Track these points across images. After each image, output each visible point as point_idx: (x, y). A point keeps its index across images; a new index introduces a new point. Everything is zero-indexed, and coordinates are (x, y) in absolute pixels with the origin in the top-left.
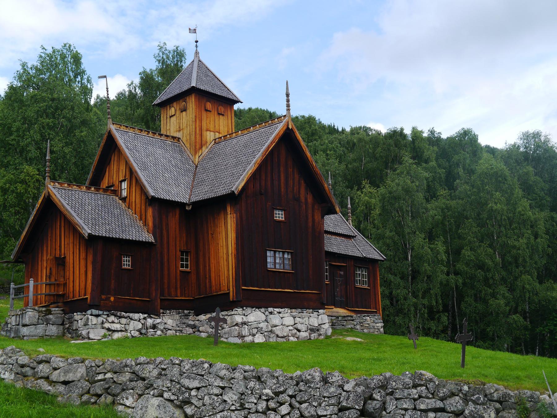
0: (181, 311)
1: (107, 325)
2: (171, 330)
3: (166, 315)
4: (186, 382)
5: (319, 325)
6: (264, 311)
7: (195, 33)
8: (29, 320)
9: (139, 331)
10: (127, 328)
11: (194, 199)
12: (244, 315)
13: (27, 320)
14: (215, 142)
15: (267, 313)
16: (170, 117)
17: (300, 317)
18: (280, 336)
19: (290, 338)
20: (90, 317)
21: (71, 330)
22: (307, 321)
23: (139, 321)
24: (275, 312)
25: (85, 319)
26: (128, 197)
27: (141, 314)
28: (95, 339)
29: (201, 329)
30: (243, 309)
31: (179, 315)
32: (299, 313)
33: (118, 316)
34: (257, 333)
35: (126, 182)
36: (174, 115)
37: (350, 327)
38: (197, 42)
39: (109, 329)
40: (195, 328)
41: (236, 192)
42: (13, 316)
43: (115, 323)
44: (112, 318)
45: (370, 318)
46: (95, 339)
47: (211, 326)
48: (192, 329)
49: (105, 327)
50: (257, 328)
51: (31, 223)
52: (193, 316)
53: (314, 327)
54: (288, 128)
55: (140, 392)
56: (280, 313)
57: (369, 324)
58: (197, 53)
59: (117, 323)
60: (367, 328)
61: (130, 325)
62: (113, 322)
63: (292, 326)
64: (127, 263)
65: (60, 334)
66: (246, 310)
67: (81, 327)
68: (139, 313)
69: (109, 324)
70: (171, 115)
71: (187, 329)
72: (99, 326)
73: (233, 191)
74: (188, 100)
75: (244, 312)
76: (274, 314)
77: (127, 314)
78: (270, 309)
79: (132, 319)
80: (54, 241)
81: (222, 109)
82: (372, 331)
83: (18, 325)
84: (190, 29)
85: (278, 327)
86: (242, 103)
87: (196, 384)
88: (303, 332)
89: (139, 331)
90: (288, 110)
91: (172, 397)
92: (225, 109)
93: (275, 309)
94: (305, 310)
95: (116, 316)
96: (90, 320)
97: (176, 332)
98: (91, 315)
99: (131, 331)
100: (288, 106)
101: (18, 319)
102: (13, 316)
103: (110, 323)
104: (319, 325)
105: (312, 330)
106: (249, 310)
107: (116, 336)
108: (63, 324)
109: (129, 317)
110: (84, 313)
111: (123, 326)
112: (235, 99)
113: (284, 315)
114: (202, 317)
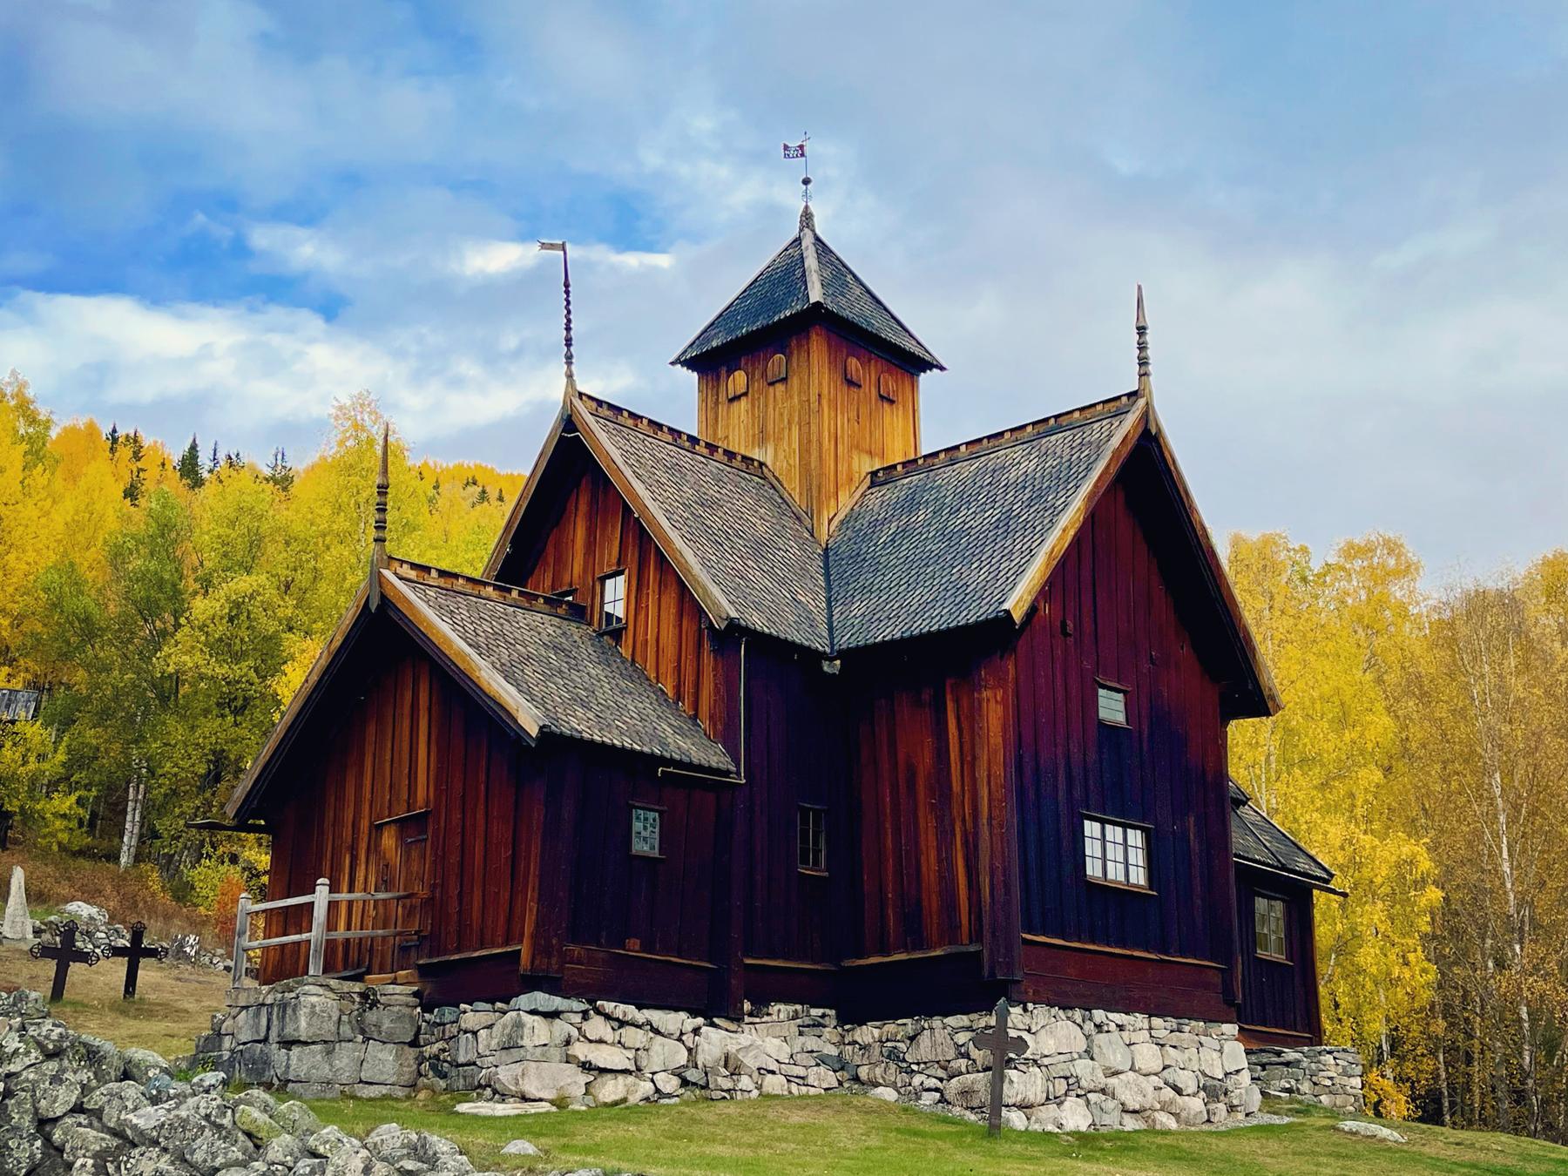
0: (799, 1007)
1: (581, 1050)
2: (773, 1072)
3: (757, 1020)
5: (1226, 1074)
6: (1079, 1020)
7: (802, 155)
8: (309, 1025)
9: (677, 1073)
10: (643, 1063)
11: (845, 641)
12: (1029, 1031)
13: (302, 1026)
14: (872, 482)
15: (1089, 1026)
16: (731, 400)
17: (1175, 1047)
18: (1131, 1109)
19: (1156, 1114)
20: (527, 1019)
21: (445, 1064)
22: (1195, 1058)
23: (679, 1040)
24: (1113, 1027)
25: (504, 1027)
26: (631, 627)
27: (683, 1015)
28: (541, 1100)
29: (863, 1073)
30: (1025, 1010)
31: (799, 1021)
32: (1172, 1031)
33: (617, 1020)
34: (1066, 1095)
35: (621, 580)
36: (745, 394)
37: (1288, 1086)
38: (806, 182)
39: (586, 1067)
40: (842, 1069)
41: (1017, 616)
42: (243, 1008)
43: (606, 1042)
44: (597, 1027)
45: (1335, 1058)
46: (541, 1100)
47: (904, 1065)
48: (835, 1071)
49: (575, 1057)
50: (1066, 1078)
51: (310, 697)
52: (835, 1027)
53: (1216, 1082)
54: (1146, 431)
56: (1121, 1028)
57: (1331, 1078)
59: (613, 1044)
60: (1327, 1090)
61: (651, 1053)
62: (601, 1041)
63: (1156, 1074)
64: (645, 835)
65: (407, 1077)
66: (1035, 1011)
67: (488, 1053)
68: (677, 1010)
69: (588, 1045)
71: (822, 1069)
72: (556, 1053)
73: (1007, 612)
74: (794, 343)
75: (1027, 1020)
76: (1108, 1032)
77: (641, 1016)
78: (1099, 1015)
79: (657, 1032)
80: (388, 757)
81: (890, 384)
82: (1339, 1100)
83: (265, 1040)
84: (786, 148)
85: (1120, 1076)
86: (942, 368)
88: (1188, 1095)
89: (677, 1073)
90: (1143, 375)
92: (897, 382)
93: (1111, 1015)
94: (1187, 1021)
95: (608, 1017)
96: (526, 1031)
97: (788, 1081)
98: (533, 1012)
99: (653, 1073)
100: (1143, 362)
101: (264, 1021)
103: (591, 1041)
104: (1226, 1074)
105: (1213, 1091)
106: (1041, 1014)
107: (610, 1090)
108: (414, 1043)
109: (649, 1023)
110: (499, 1005)
111: (631, 1054)
112: (927, 357)
113: (1135, 1037)
114: (868, 1033)
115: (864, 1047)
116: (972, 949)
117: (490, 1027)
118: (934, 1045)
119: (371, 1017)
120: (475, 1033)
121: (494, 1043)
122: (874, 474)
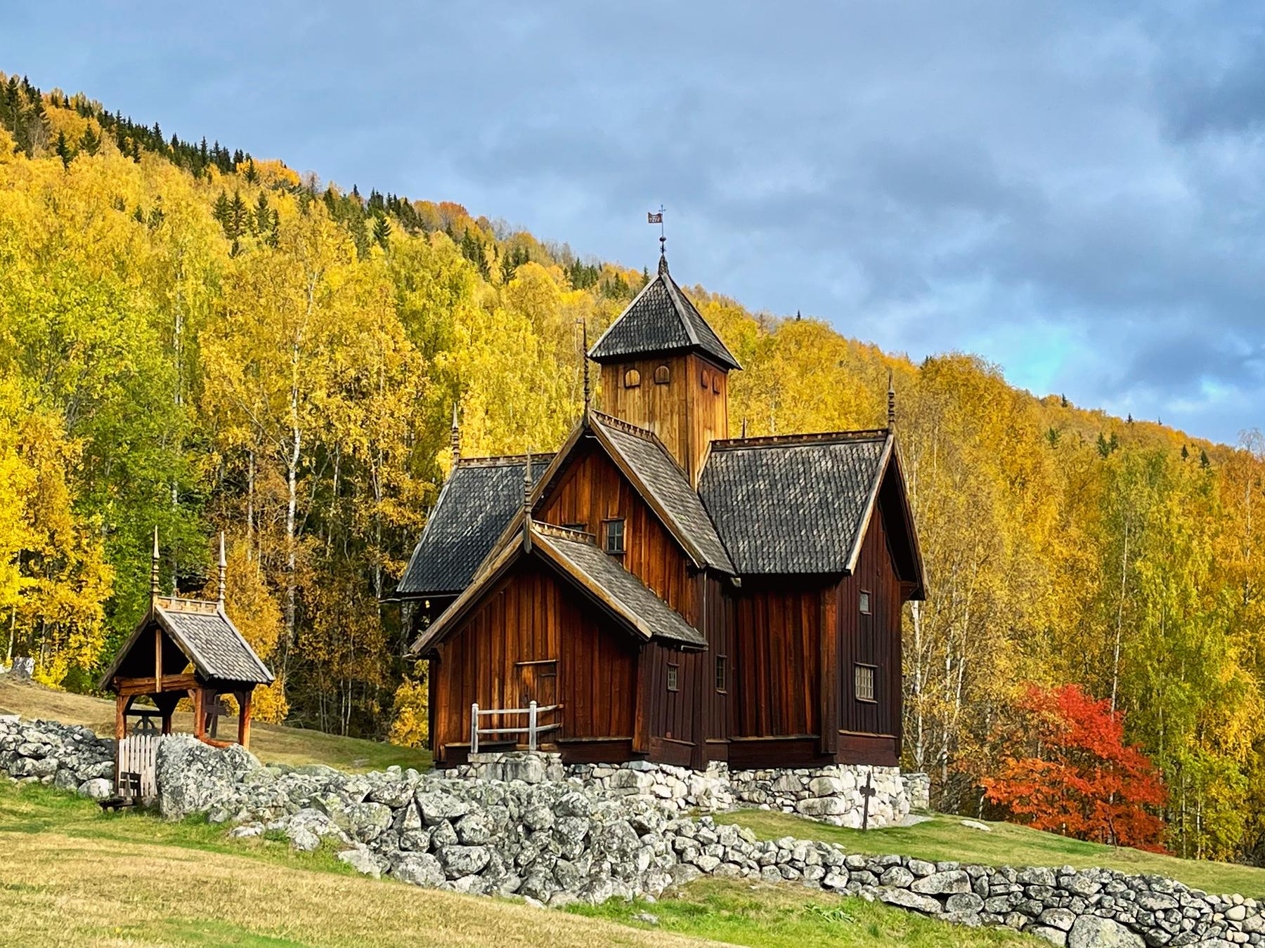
4: (1151, 902)
7: (660, 221)
16: (627, 388)
25: (621, 777)
29: (745, 796)
36: (639, 386)
38: (662, 240)
42: (482, 764)
55: (1081, 912)
58: (663, 263)
70: (628, 384)
84: (650, 215)
87: (1166, 904)
91: (1133, 920)
96: (639, 780)
102: (482, 764)
114: (747, 775)
115: (745, 783)
116: (815, 737)
117: (610, 776)
118: (789, 783)
119: (549, 769)
120: (601, 779)
121: (614, 784)
122: (714, 443)
